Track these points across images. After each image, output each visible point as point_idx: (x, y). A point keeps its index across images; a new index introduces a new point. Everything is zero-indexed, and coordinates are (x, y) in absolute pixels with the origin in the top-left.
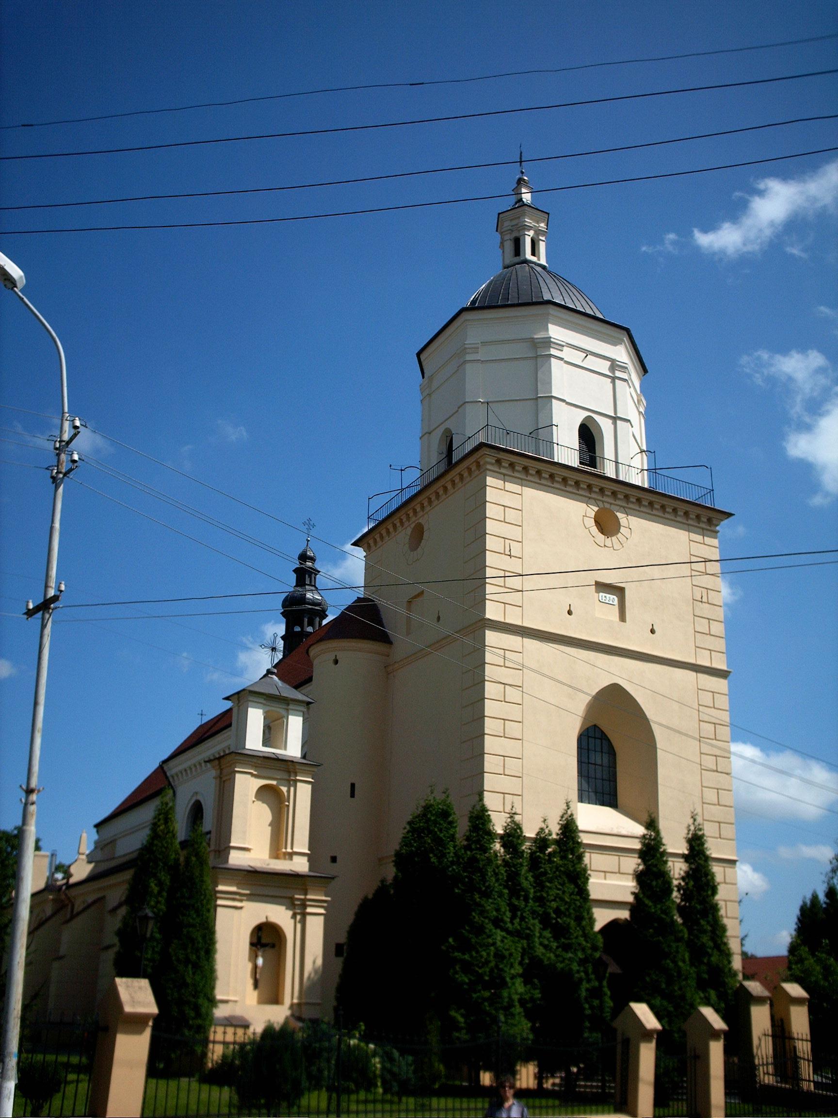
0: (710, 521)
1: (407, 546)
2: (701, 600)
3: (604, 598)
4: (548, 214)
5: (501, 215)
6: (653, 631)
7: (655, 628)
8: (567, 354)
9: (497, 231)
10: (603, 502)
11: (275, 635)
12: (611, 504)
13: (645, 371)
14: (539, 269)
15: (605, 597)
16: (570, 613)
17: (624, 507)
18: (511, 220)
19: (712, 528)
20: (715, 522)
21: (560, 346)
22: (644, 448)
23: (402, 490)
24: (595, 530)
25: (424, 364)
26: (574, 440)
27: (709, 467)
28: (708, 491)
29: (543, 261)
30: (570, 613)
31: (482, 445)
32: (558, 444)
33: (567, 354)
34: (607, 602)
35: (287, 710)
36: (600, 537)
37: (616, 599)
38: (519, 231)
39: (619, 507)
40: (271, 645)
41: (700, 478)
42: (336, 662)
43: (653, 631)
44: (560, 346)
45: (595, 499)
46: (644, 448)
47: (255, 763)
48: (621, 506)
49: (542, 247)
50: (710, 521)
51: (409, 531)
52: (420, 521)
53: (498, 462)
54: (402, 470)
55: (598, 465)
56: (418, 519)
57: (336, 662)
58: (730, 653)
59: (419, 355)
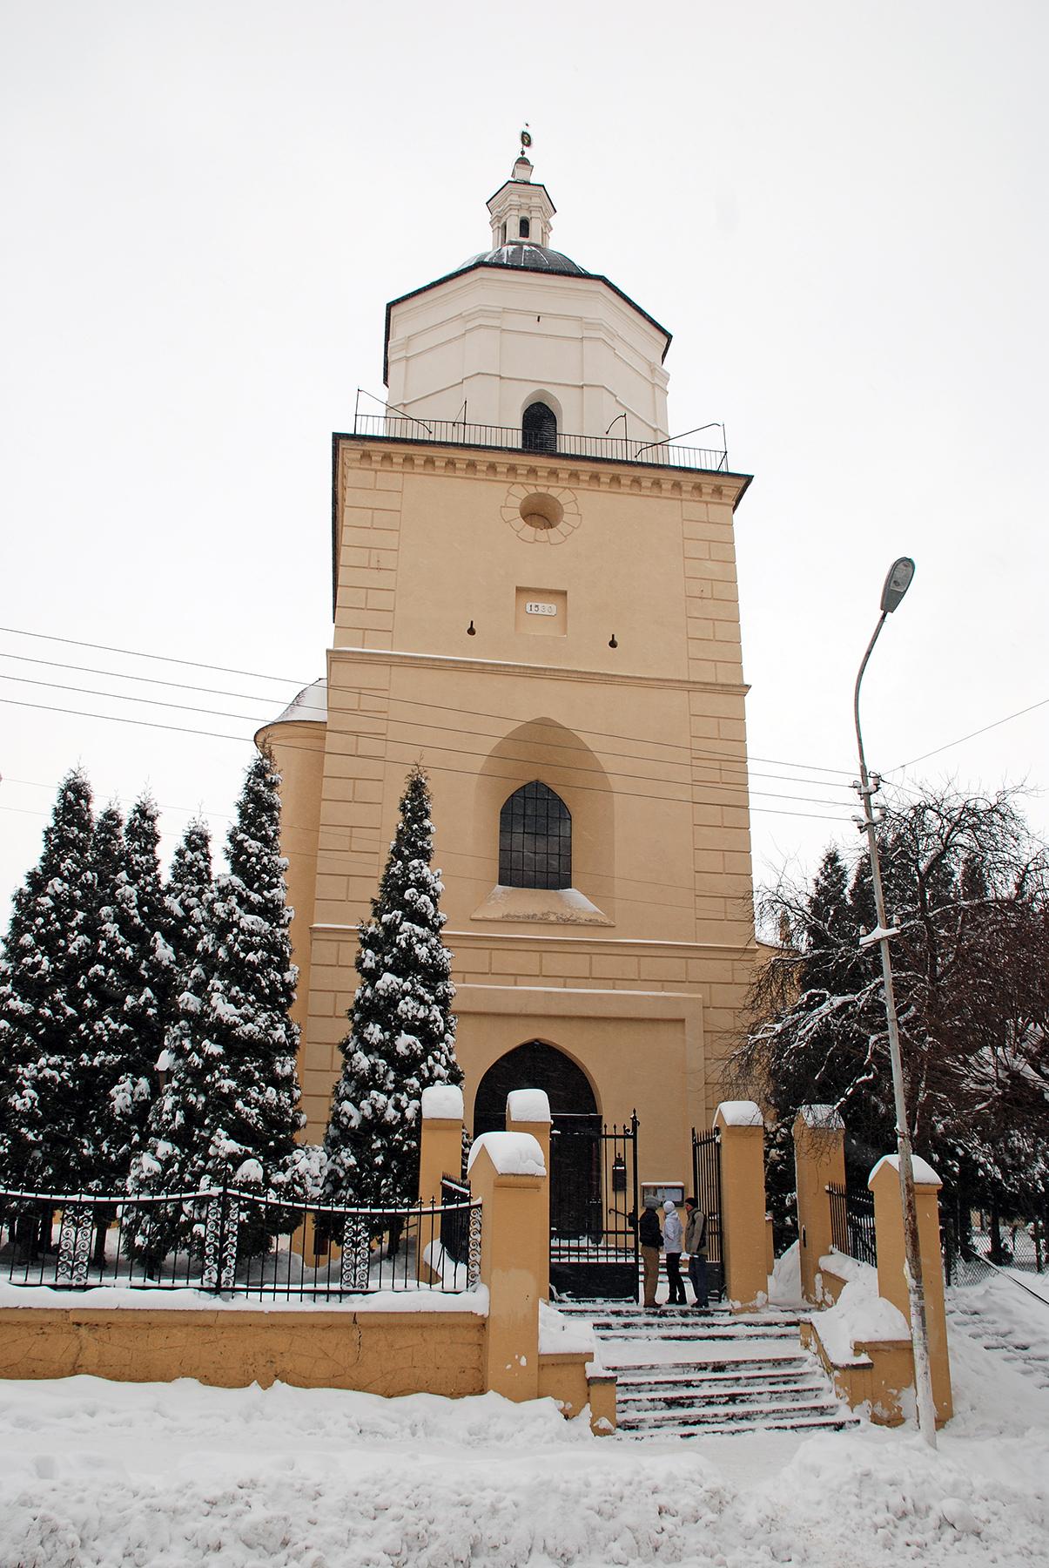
3: (533, 608)
6: (613, 644)
7: (615, 639)
10: (535, 486)
12: (549, 487)
15: (537, 606)
17: (569, 489)
27: (721, 424)
30: (471, 631)
32: (465, 424)
34: (539, 612)
36: (543, 534)
39: (562, 490)
41: (712, 439)
45: (522, 484)
48: (565, 488)
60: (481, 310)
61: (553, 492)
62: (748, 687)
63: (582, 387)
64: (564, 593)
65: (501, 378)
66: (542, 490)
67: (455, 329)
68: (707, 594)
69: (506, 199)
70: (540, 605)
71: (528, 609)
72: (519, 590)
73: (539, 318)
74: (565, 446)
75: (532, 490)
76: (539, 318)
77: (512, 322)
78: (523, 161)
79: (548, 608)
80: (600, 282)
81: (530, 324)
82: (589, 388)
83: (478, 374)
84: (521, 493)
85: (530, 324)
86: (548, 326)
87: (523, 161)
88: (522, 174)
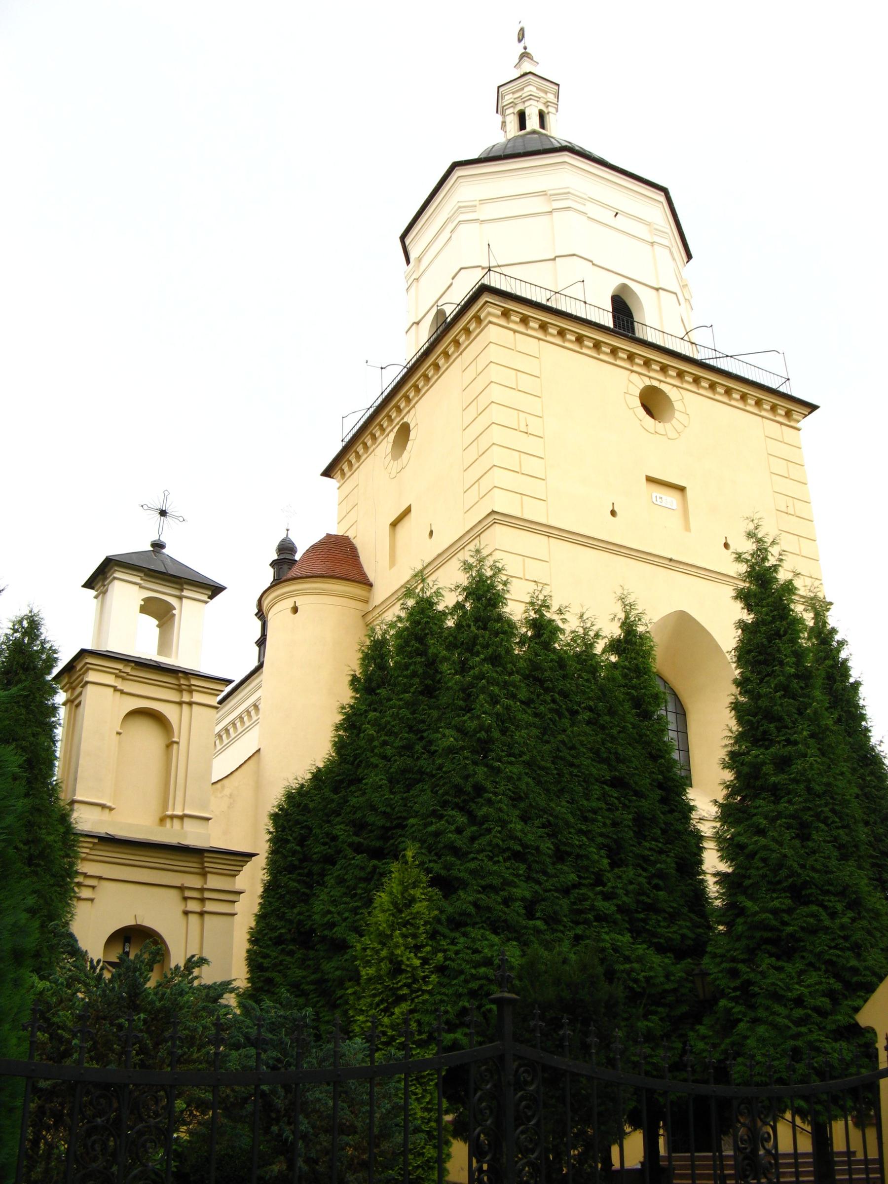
0: (788, 414)
1: (390, 456)
2: (784, 509)
4: (558, 85)
5: (501, 89)
9: (497, 112)
10: (650, 377)
11: (166, 493)
12: (661, 381)
16: (613, 513)
18: (513, 93)
19: (792, 424)
20: (795, 416)
24: (641, 412)
25: (409, 248)
28: (784, 380)
30: (613, 513)
32: (585, 303)
33: (593, 210)
35: (180, 598)
37: (675, 502)
38: (524, 102)
40: (159, 507)
42: (295, 610)
47: (120, 671)
48: (674, 386)
50: (788, 414)
51: (392, 436)
52: (405, 420)
53: (506, 314)
54: (382, 368)
56: (403, 418)
57: (295, 610)
59: (403, 238)
60: (569, 193)
61: (663, 386)
62: (831, 604)
63: (657, 289)
64: (682, 489)
65: (593, 264)
66: (655, 383)
67: (539, 204)
68: (791, 511)
69: (523, 89)
70: (664, 497)
71: (654, 500)
72: (650, 480)
73: (617, 214)
75: (648, 382)
76: (617, 214)
77: (593, 210)
78: (525, 55)
79: (671, 499)
80: (663, 194)
82: (665, 292)
83: (574, 255)
84: (639, 383)
85: (607, 216)
87: (525, 55)
88: (527, 67)
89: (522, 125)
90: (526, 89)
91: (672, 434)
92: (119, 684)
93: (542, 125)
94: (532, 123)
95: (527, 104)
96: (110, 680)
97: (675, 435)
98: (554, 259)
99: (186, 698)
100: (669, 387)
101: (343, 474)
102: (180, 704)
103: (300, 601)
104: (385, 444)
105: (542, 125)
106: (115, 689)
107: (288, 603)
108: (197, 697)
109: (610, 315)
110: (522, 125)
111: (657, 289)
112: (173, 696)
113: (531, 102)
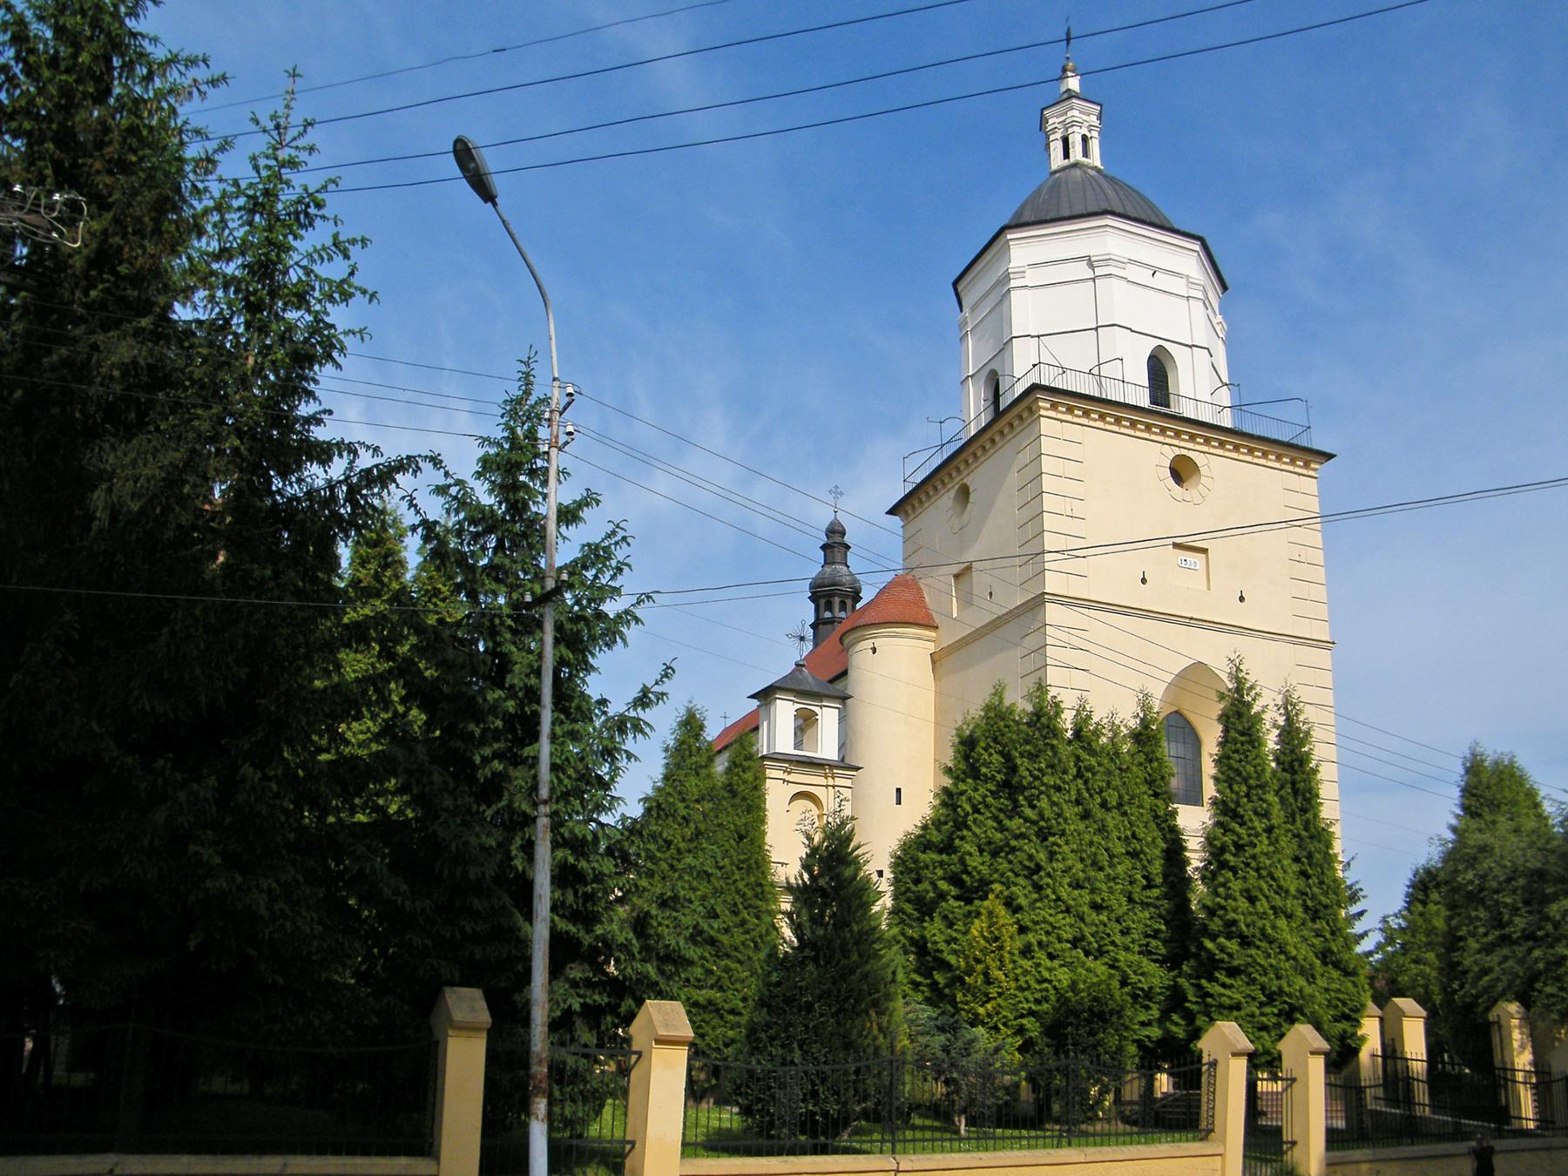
6: (1242, 599)
8: (1133, 273)
13: (1224, 288)
14: (1093, 173)
16: (1144, 581)
21: (1122, 263)
22: (1226, 380)
23: (943, 445)
25: (962, 295)
26: (1143, 378)
29: (1098, 163)
30: (1144, 581)
31: (1035, 388)
33: (1133, 273)
35: (821, 707)
43: (1242, 599)
44: (1122, 263)
46: (1226, 380)
49: (1095, 146)
51: (953, 493)
55: (1172, 404)
58: (1332, 620)
59: (955, 284)
63: (1190, 346)
64: (1204, 551)
66: (1184, 452)
74: (1188, 411)
75: (1178, 452)
81: (1143, 276)
84: (1171, 453)
85: (1143, 276)
86: (1161, 281)
89: (1066, 155)
90: (1069, 114)
91: (1198, 499)
92: (785, 776)
93: (1086, 154)
94: (1076, 153)
95: (1070, 131)
96: (780, 774)
97: (1199, 500)
98: (1096, 329)
99: (830, 781)
100: (1200, 455)
101: (906, 513)
102: (827, 786)
103: (878, 642)
104: (945, 500)
105: (1086, 154)
106: (784, 781)
107: (868, 644)
108: (838, 781)
109: (1147, 391)
110: (1066, 155)
111: (1190, 346)
112: (822, 781)
113: (1075, 129)
